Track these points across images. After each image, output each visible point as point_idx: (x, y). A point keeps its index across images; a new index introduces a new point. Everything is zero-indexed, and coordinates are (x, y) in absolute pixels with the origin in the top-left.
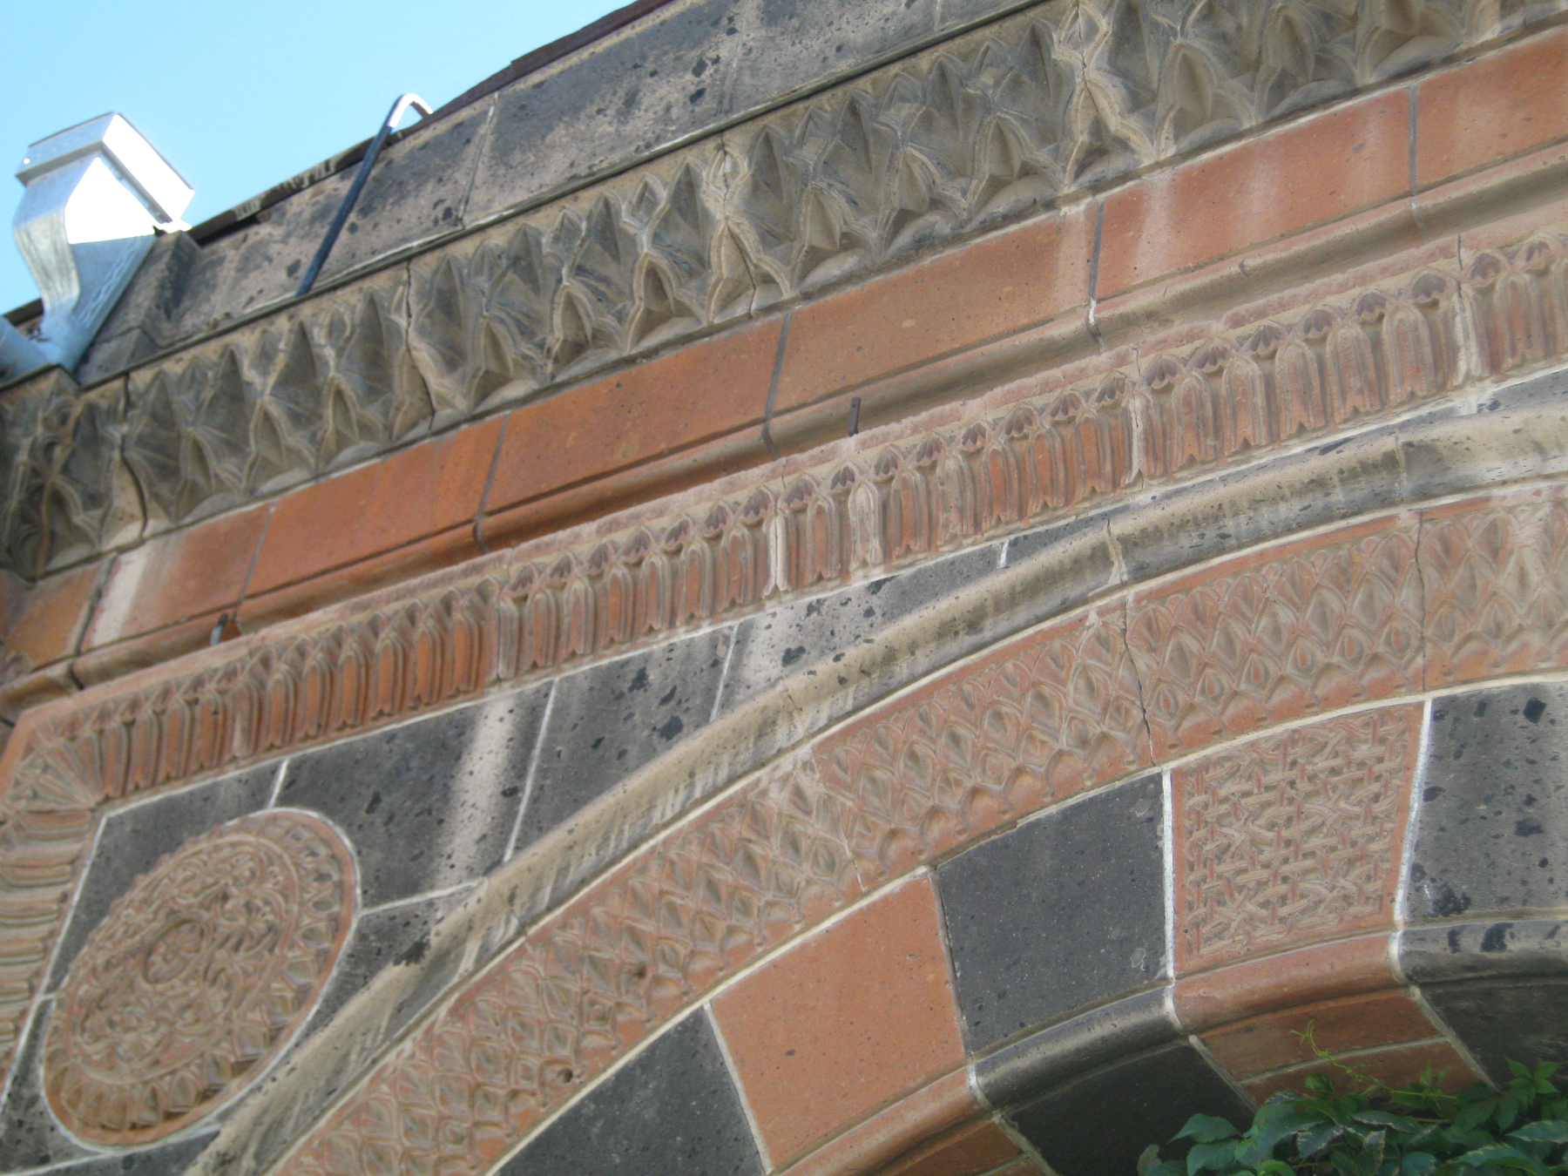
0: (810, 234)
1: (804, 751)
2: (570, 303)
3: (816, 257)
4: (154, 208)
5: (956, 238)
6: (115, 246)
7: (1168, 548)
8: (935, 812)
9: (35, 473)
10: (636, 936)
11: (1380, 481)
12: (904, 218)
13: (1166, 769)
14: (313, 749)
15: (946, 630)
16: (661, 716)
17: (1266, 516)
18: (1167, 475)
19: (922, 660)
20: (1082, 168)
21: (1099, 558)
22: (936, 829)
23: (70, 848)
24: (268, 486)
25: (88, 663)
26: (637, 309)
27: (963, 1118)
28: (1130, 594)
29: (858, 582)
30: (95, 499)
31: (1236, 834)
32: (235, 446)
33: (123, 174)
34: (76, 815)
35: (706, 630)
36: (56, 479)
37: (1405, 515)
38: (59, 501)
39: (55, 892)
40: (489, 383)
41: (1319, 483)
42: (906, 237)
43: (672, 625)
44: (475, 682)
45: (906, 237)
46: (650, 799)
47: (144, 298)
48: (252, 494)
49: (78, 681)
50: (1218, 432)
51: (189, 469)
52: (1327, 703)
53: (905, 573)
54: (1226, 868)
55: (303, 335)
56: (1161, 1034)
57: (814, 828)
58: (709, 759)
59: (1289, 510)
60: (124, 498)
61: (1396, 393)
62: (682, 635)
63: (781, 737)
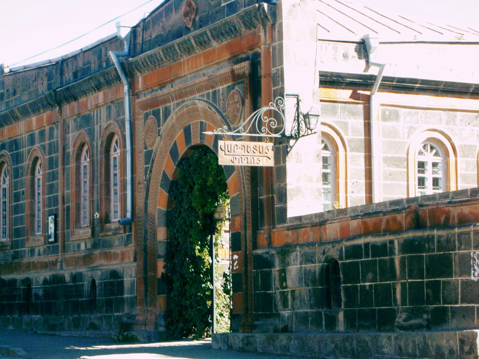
6: (127, 35)
13: (191, 123)
21: (183, 106)
27: (187, 151)
30: (134, 71)
47: (132, 39)
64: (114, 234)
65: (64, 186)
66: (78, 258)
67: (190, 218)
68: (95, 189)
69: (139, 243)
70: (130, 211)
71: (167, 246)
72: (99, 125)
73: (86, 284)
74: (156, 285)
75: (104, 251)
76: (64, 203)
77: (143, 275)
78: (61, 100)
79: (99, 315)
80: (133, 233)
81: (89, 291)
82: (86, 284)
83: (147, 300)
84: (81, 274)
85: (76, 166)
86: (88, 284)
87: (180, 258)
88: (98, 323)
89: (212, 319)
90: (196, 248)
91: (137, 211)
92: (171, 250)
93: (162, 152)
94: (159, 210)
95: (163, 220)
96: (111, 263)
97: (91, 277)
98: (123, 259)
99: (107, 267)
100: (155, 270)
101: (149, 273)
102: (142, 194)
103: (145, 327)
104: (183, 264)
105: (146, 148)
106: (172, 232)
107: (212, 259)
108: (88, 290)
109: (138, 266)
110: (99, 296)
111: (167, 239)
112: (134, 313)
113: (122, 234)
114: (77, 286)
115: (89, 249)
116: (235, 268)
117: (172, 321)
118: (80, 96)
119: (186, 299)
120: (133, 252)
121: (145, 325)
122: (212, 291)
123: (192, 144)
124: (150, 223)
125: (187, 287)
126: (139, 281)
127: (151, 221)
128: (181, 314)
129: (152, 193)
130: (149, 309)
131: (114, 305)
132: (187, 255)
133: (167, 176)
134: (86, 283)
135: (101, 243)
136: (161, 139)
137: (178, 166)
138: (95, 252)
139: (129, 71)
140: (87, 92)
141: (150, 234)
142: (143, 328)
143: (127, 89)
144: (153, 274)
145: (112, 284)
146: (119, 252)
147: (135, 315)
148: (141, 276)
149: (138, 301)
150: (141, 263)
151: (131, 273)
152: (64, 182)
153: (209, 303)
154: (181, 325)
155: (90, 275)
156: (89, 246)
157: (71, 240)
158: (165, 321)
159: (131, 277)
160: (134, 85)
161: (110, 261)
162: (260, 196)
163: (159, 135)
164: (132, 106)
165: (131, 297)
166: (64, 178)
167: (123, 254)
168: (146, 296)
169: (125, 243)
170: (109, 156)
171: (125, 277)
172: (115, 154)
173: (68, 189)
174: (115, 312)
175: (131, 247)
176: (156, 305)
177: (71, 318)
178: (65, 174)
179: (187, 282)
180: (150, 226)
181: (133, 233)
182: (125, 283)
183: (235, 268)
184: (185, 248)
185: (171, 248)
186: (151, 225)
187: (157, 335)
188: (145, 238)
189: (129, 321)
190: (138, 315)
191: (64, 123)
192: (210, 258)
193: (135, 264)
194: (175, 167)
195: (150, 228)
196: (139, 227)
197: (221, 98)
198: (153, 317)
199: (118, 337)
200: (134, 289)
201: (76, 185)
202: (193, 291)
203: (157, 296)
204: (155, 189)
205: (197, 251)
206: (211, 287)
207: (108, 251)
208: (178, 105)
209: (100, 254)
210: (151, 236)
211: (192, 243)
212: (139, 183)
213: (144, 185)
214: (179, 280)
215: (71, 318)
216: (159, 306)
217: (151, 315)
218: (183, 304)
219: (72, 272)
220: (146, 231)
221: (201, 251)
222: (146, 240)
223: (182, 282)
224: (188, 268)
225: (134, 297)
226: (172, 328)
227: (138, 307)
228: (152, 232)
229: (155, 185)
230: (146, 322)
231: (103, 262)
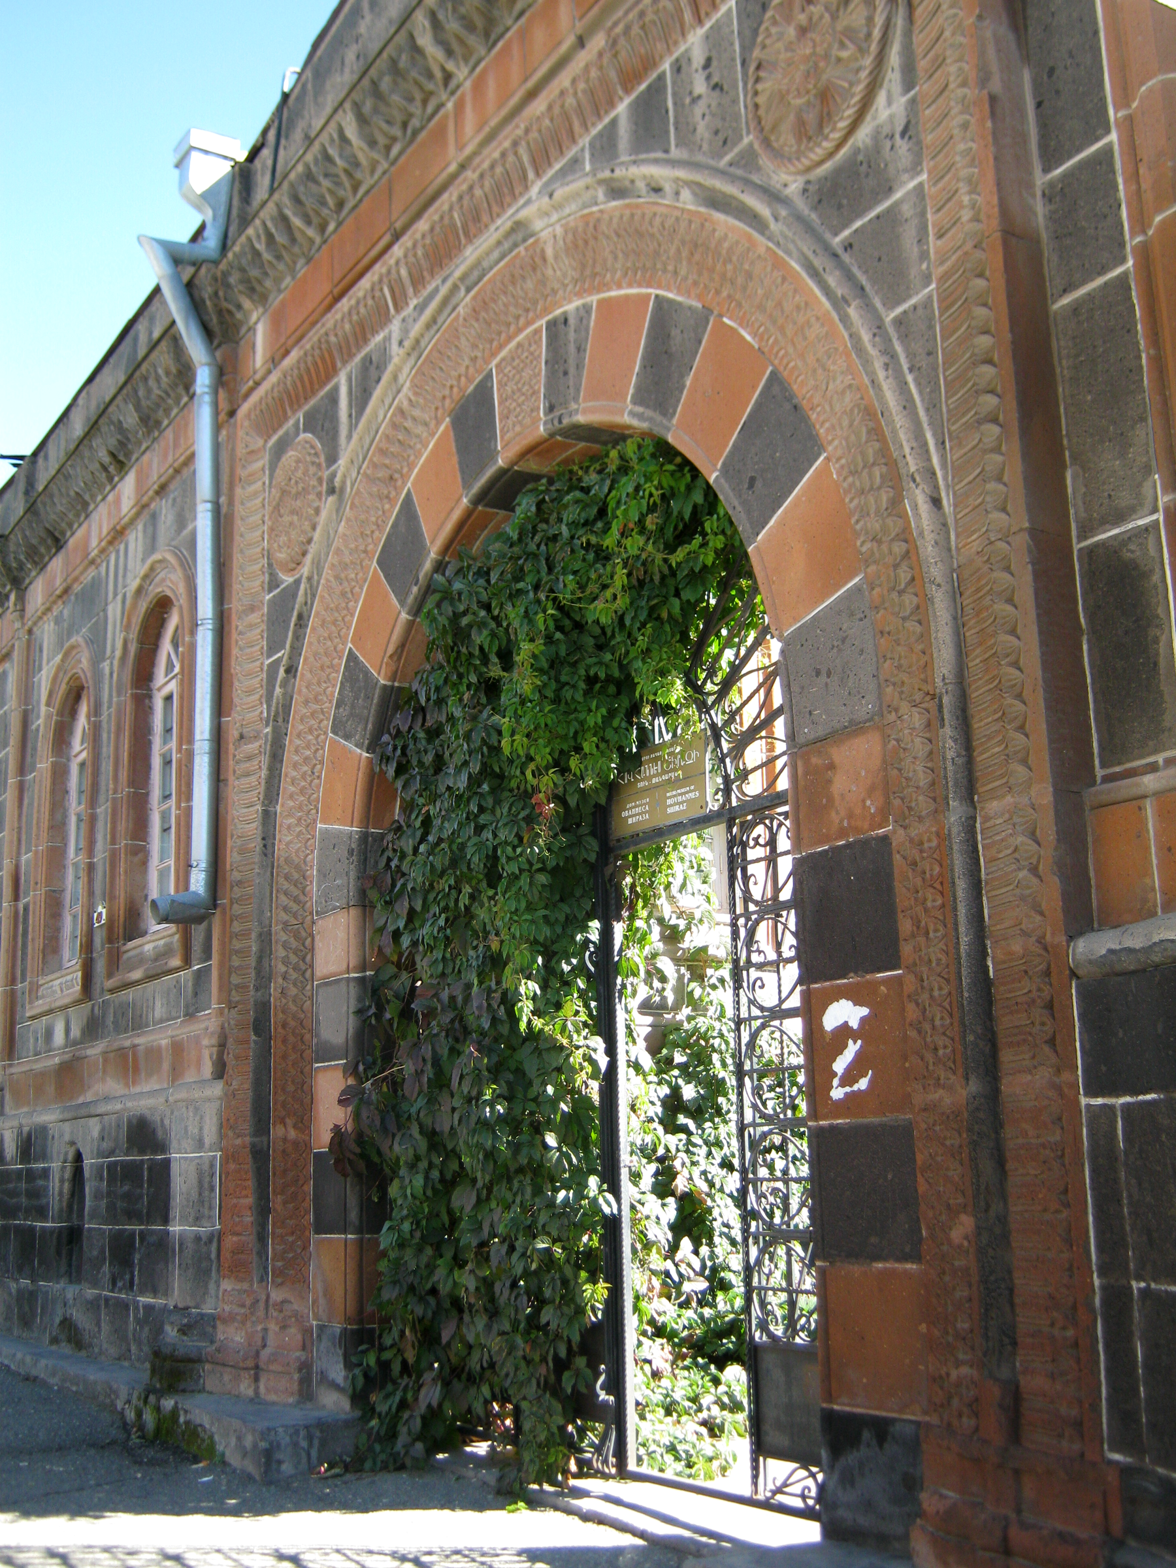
0: (382, 141)
2: (329, 190)
3: (388, 148)
4: (226, 158)
5: (422, 128)
6: (218, 184)
8: (444, 398)
9: (216, 305)
10: (386, 466)
12: (405, 125)
14: (306, 408)
15: (428, 326)
19: (427, 339)
20: (446, 85)
21: (455, 288)
22: (447, 402)
23: (260, 464)
24: (283, 286)
25: (258, 377)
26: (347, 185)
27: (468, 514)
29: (411, 306)
30: (239, 307)
32: (266, 274)
33: (206, 152)
34: (259, 450)
36: (225, 305)
38: (229, 312)
39: (260, 483)
40: (322, 228)
41: (499, 243)
42: (409, 132)
45: (409, 132)
46: (375, 414)
47: (236, 202)
48: (280, 291)
49: (258, 384)
51: (258, 288)
55: (264, 224)
56: (502, 472)
57: (416, 413)
58: (385, 394)
59: (496, 255)
60: (247, 304)
63: (401, 379)
64: (150, 977)
65: (19, 840)
66: (43, 1074)
67: (487, 835)
68: (100, 825)
69: (235, 997)
70: (203, 865)
71: (360, 999)
72: (119, 597)
73: (57, 1167)
74: (310, 1187)
75: (116, 1045)
76: (16, 897)
77: (248, 1140)
78: (21, 567)
79: (90, 1293)
80: (214, 961)
81: (66, 1197)
82: (57, 1167)
83: (262, 1252)
84: (43, 1130)
85: (54, 765)
86: (63, 1168)
87: (427, 1051)
88: (87, 1326)
89: (617, 1385)
90: (522, 990)
91: (232, 857)
92: (379, 1016)
93: (345, 567)
94: (326, 835)
95: (345, 880)
96: (137, 1089)
97: (72, 1143)
98: (176, 1072)
99: (119, 1106)
100: (304, 1115)
101: (277, 1131)
102: (253, 779)
103: (256, 1379)
104: (440, 1082)
105: (273, 583)
106: (381, 930)
107: (611, 1051)
108: (61, 1194)
109: (230, 1096)
110: (93, 1217)
111: (363, 967)
112: (207, 1309)
113: (177, 970)
114: (31, 1175)
115: (75, 1043)
116: (837, 1093)
117: (384, 1366)
118: (70, 525)
119: (459, 1262)
120: (214, 1041)
121: (257, 1371)
122: (612, 1225)
123: (500, 462)
124: (284, 900)
125: (463, 1199)
126: (232, 1166)
127: (286, 893)
128: (429, 1338)
129: (295, 766)
130: (276, 1295)
131: (137, 1256)
132: (466, 1031)
133: (367, 673)
134: (55, 1165)
135: (110, 1018)
136: (339, 509)
137: (416, 611)
138: (89, 1052)
139: (220, 312)
140: (87, 497)
141: (281, 953)
142: (245, 1388)
143: (207, 382)
144: (292, 1134)
145: (130, 1172)
146: (164, 1042)
147: (213, 1318)
148: (238, 1141)
149: (226, 1254)
150: (242, 1081)
151: (201, 1129)
152: (20, 828)
153: (596, 1293)
154: (431, 1394)
155: (67, 1138)
156: (76, 1032)
157: (28, 1014)
158: (348, 1365)
159: (200, 1145)
160: (235, 371)
161: (134, 1083)
162: (1083, 535)
163: (332, 491)
164: (224, 456)
165: (198, 1238)
166: (20, 816)
167: (177, 1048)
168: (262, 1238)
169: (187, 1006)
170: (150, 697)
171: (174, 1145)
172: (165, 683)
173: (28, 851)
174: (142, 1292)
175: (209, 1022)
176: (305, 1281)
177: (13, 1286)
178: (26, 802)
179: (461, 1176)
180: (284, 916)
181: (214, 961)
182: (175, 1169)
183: (837, 1093)
184: (453, 998)
185: (381, 1009)
186: (285, 909)
187: (310, 1438)
188: (259, 969)
189: (190, 1344)
190: (224, 1321)
191: (29, 641)
192: (598, 1043)
193: (217, 1089)
194: (404, 616)
195: (286, 924)
196: (237, 927)
197: (700, 86)
198: (293, 1335)
199: (139, 1414)
200: (211, 1199)
201: (51, 827)
202: (501, 1220)
203: (314, 1237)
204: (308, 747)
205: (526, 1008)
206: (608, 1204)
207: (127, 1043)
209: (105, 1053)
210: (286, 961)
211: (496, 962)
212: (242, 737)
213: (262, 742)
214: (423, 1165)
215: (13, 1286)
216: (320, 1287)
217: (284, 1327)
218: (444, 1289)
219: (21, 1127)
220: (266, 939)
221: (549, 1005)
222: (263, 978)
223: (435, 1174)
224: (473, 1099)
225: (212, 1235)
226: (383, 1404)
227: (227, 1285)
228: (294, 944)
229: (311, 731)
230: (257, 1354)
231: (112, 1086)
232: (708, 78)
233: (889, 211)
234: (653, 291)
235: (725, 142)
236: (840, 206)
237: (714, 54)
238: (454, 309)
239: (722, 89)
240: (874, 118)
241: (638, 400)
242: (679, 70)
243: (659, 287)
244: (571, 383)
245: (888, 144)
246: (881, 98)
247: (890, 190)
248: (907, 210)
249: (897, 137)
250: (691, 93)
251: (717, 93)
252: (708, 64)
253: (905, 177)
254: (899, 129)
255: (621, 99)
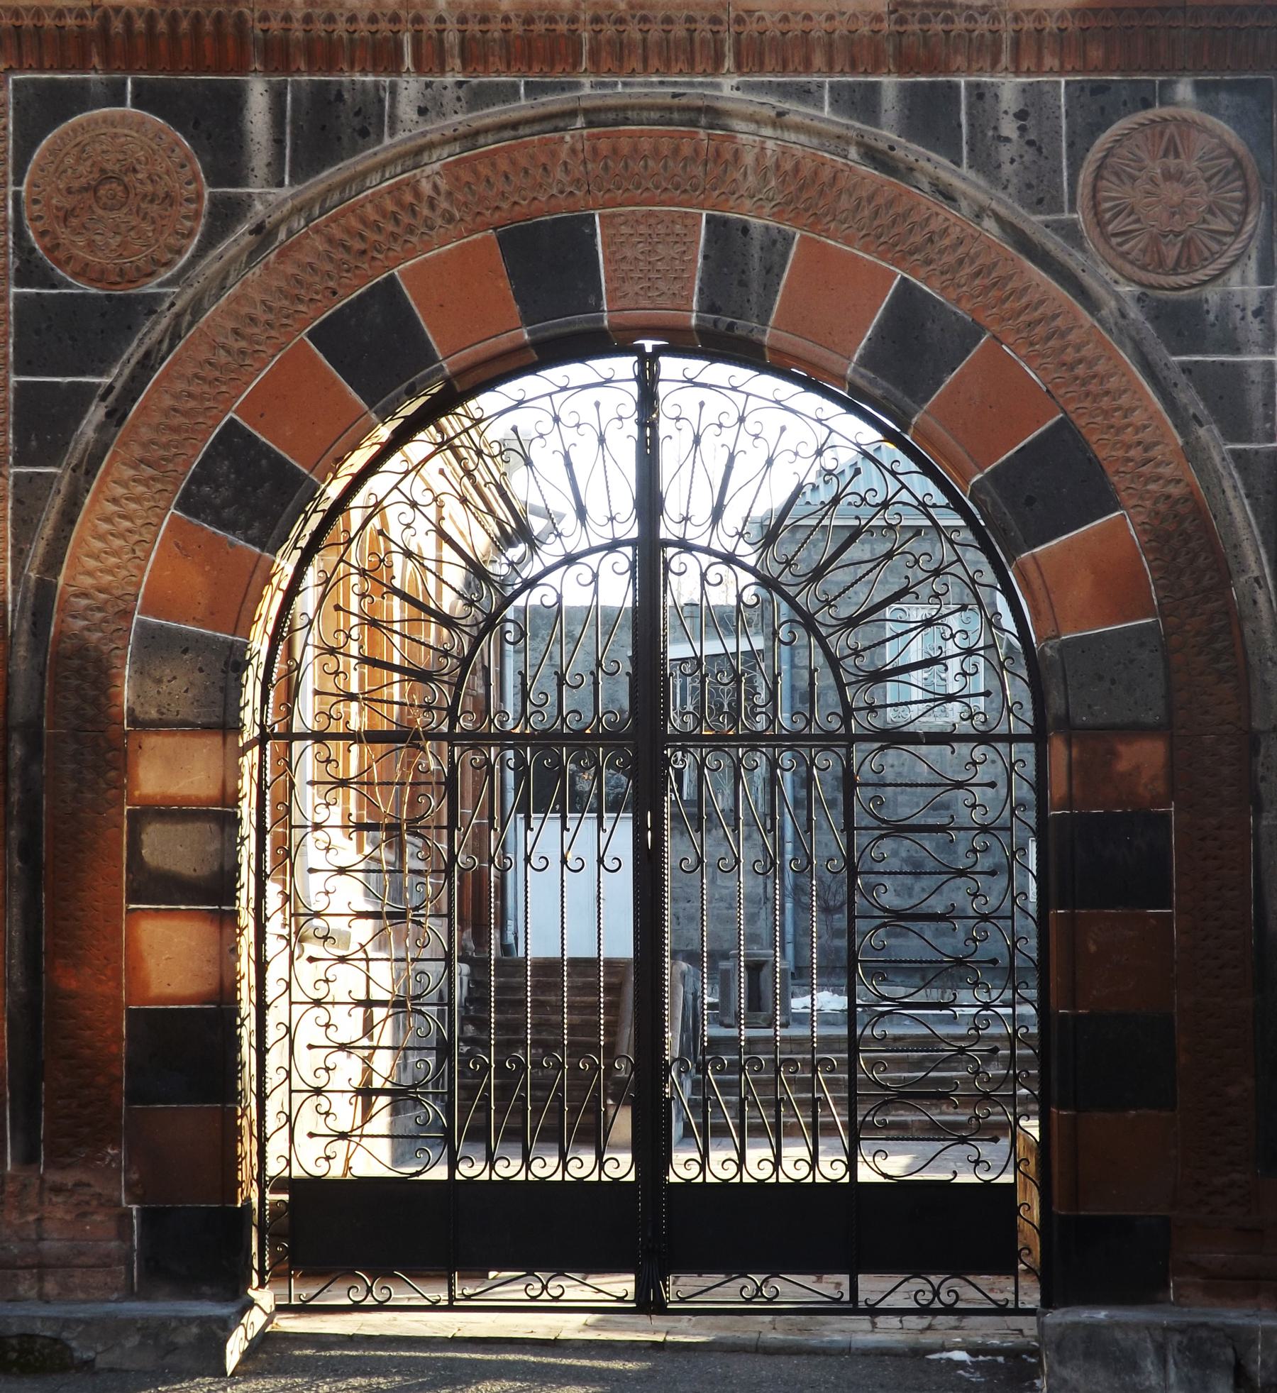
1: (437, 166)
7: (603, 117)
10: (362, 237)
11: (693, 115)
16: (356, 122)
17: (645, 114)
18: (597, 73)
19: (490, 138)
22: (497, 216)
28: (585, 132)
31: (629, 253)
35: (370, 78)
37: (702, 134)
43: (352, 67)
44: (243, 69)
50: (621, 60)
52: (663, 204)
53: (475, 81)
54: (625, 267)
59: (654, 115)
61: (699, 68)
62: (358, 77)
63: (425, 158)
197: (1009, 128)
208: (479, 97)
232: (1022, 129)
233: (1234, 364)
234: (900, 274)
235: (1040, 201)
236: (1179, 334)
237: (1030, 110)
238: (556, 130)
239: (1039, 150)
240: (1225, 284)
241: (865, 361)
242: (981, 96)
243: (913, 272)
244: (753, 298)
245: (1239, 314)
246: (1235, 275)
247: (1237, 351)
248: (1255, 374)
249: (1249, 313)
250: (995, 128)
251: (1032, 150)
252: (1021, 115)
253: (1256, 349)
254: (1251, 309)
255: (889, 72)
